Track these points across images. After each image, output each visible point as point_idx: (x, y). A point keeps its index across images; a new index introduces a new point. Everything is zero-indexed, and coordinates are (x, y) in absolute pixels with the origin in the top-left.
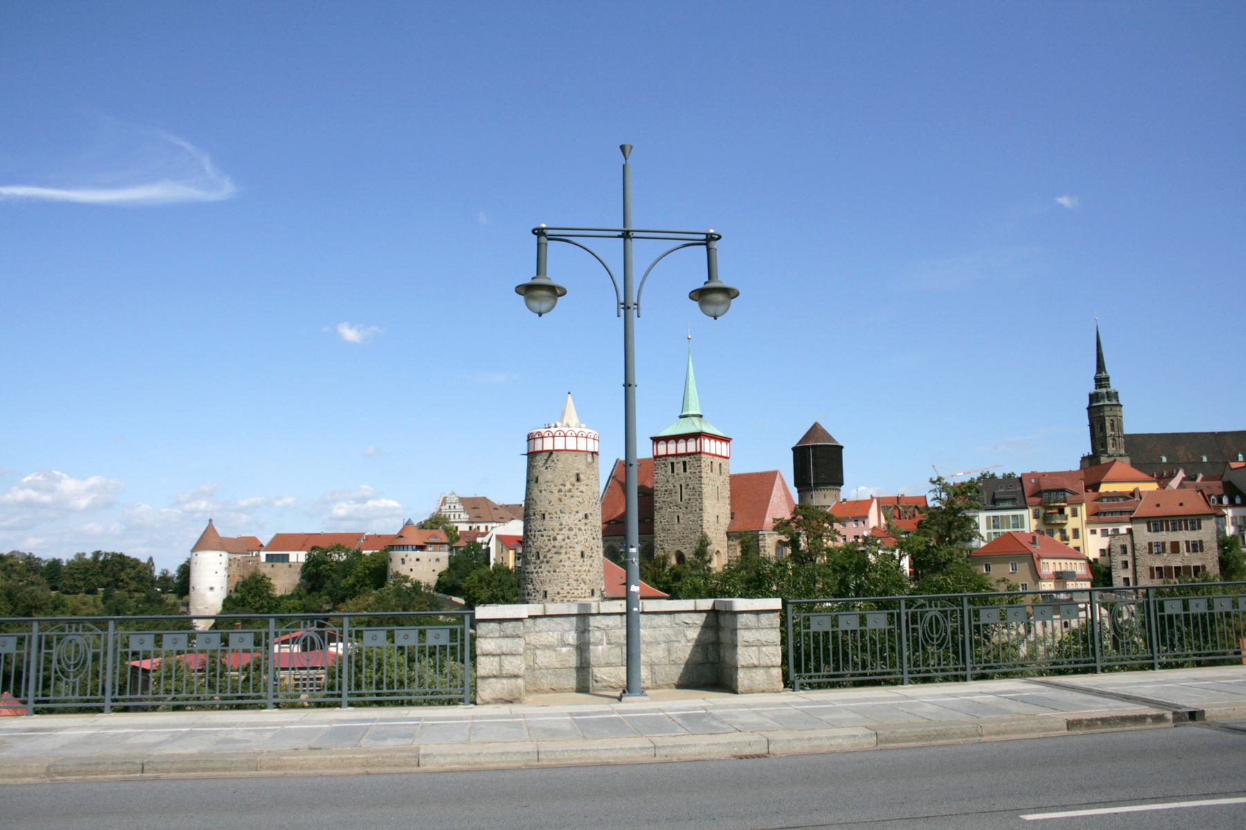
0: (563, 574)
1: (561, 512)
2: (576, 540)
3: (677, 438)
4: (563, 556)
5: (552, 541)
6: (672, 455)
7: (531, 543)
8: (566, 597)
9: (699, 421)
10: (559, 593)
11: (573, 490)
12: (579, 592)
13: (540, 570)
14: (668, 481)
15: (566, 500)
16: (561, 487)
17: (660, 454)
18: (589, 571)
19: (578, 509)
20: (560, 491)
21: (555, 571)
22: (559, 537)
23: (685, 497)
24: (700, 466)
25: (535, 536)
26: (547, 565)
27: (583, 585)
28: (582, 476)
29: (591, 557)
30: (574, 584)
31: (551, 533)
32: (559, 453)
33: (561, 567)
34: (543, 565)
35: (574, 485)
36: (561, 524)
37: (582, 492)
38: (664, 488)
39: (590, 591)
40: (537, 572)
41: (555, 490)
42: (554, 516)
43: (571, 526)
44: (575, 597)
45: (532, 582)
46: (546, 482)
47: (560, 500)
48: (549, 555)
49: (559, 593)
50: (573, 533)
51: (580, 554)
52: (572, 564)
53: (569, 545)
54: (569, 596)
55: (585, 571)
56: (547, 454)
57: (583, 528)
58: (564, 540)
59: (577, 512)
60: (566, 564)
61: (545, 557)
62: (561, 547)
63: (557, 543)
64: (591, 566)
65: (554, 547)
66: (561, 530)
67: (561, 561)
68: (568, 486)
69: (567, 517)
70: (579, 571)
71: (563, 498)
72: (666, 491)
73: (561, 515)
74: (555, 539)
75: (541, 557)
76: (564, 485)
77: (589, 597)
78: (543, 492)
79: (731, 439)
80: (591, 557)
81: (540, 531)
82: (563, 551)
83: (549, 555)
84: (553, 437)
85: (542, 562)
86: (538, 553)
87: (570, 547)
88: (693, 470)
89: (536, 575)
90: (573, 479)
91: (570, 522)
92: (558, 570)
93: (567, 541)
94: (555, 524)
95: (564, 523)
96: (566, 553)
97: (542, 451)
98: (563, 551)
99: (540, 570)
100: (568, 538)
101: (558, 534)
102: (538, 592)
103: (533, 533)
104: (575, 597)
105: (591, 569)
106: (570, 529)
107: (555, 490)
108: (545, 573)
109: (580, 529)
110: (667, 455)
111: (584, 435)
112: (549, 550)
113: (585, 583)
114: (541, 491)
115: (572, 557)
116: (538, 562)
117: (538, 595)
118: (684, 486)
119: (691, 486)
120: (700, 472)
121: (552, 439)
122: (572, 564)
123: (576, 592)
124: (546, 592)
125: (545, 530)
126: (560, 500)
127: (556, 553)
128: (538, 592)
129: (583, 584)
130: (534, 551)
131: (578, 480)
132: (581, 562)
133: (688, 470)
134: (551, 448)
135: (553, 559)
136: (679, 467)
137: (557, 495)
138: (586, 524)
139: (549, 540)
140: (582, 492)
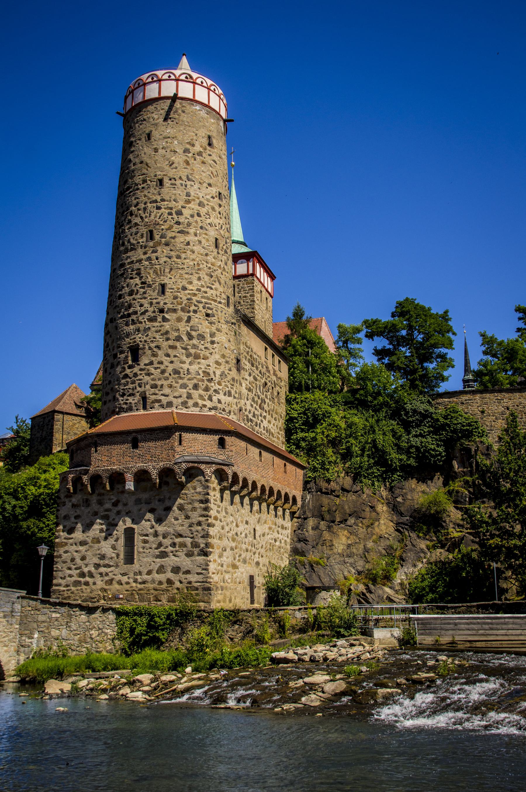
0: (192, 263)
2: (208, 221)
4: (190, 238)
5: (175, 216)
7: (138, 220)
8: (195, 295)
10: (184, 288)
11: (204, 155)
12: (213, 292)
13: (154, 256)
15: (196, 165)
16: (188, 146)
20: (186, 151)
21: (179, 257)
22: (186, 212)
24: (253, 289)
25: (145, 209)
26: (168, 248)
27: (217, 285)
28: (214, 141)
30: (207, 278)
31: (173, 204)
32: (185, 103)
33: (188, 252)
34: (159, 249)
35: (205, 149)
36: (188, 195)
40: (149, 259)
41: (180, 150)
42: (178, 182)
44: (208, 298)
45: (139, 274)
46: (165, 138)
47: (187, 163)
48: (170, 234)
52: (202, 251)
53: (200, 224)
56: (169, 101)
58: (192, 216)
59: (210, 185)
60: (195, 248)
62: (189, 224)
63: (182, 219)
65: (178, 223)
66: (188, 202)
68: (198, 148)
71: (191, 161)
73: (189, 183)
74: (179, 213)
75: (157, 237)
76: (193, 145)
78: (160, 151)
81: (156, 201)
82: (192, 231)
84: (177, 80)
85: (159, 243)
86: (151, 232)
87: (201, 228)
89: (147, 263)
90: (205, 141)
91: (201, 195)
92: (183, 256)
93: (196, 217)
94: (180, 192)
95: (192, 194)
96: (196, 235)
97: (160, 99)
98: (192, 231)
99: (154, 256)
100: (199, 215)
101: (183, 207)
102: (150, 286)
103: (142, 206)
104: (208, 298)
106: (201, 204)
107: (180, 150)
108: (163, 260)
109: (213, 209)
112: (170, 228)
114: (156, 150)
115: (203, 241)
116: (151, 244)
117: (149, 291)
120: (252, 296)
121: (174, 83)
123: (210, 292)
124: (163, 286)
125: (163, 200)
128: (150, 286)
129: (217, 283)
130: (144, 230)
131: (210, 144)
132: (216, 253)
133: (237, 294)
135: (177, 240)
139: (170, 214)
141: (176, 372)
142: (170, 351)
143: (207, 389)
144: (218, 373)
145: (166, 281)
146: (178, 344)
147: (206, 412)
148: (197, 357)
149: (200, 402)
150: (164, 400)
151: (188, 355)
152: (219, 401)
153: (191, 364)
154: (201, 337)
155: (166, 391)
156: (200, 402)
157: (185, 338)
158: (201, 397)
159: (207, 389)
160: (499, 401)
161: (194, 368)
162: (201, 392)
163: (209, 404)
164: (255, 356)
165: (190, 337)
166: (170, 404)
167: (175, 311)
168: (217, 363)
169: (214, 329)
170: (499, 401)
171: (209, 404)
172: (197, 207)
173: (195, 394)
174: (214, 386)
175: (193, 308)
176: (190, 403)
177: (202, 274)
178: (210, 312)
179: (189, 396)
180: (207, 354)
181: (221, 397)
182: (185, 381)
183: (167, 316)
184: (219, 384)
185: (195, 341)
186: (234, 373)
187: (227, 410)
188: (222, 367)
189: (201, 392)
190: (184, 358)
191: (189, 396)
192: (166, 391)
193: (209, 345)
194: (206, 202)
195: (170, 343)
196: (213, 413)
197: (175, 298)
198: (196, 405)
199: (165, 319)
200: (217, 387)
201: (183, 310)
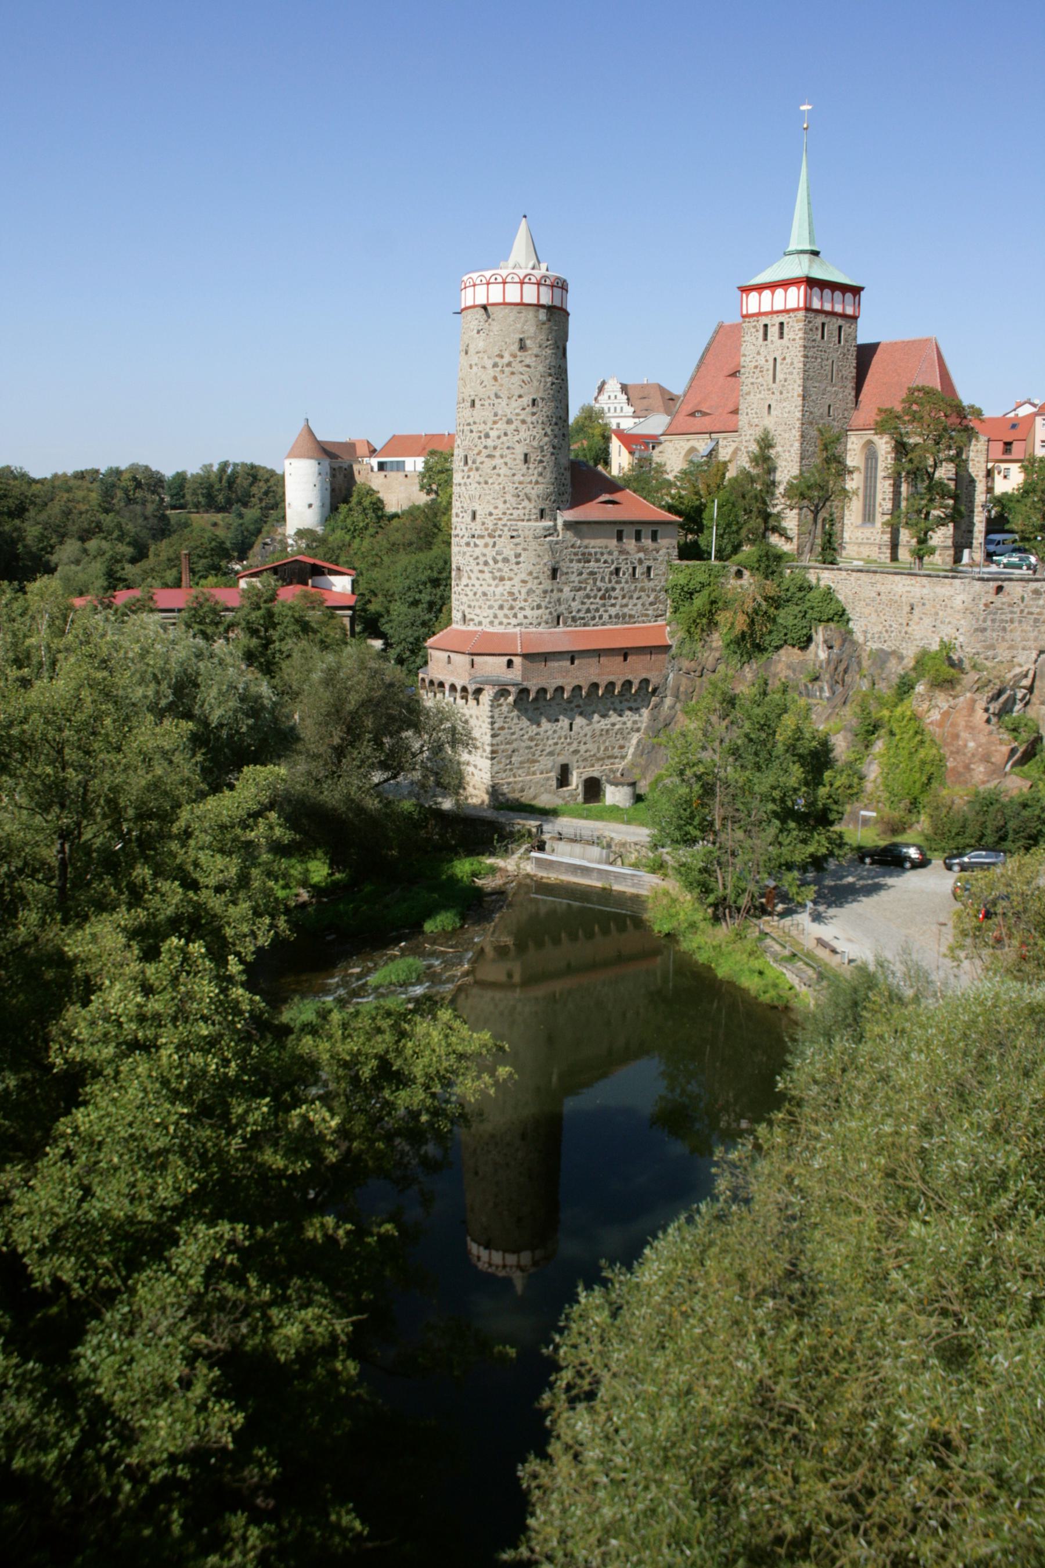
1: (497, 396)
2: (516, 438)
3: (772, 286)
4: (498, 461)
6: (766, 314)
9: (810, 261)
10: (491, 514)
12: (521, 512)
14: (759, 353)
16: (497, 360)
17: (750, 312)
18: (537, 483)
19: (522, 392)
21: (486, 483)
22: (493, 434)
23: (780, 376)
27: (526, 503)
29: (541, 462)
30: (513, 501)
31: (482, 427)
35: (515, 356)
36: (496, 415)
37: (528, 366)
38: (753, 364)
39: (537, 511)
43: (509, 416)
47: (495, 379)
48: (479, 459)
49: (491, 514)
50: (513, 427)
51: (522, 457)
54: (505, 518)
55: (531, 482)
57: (529, 419)
58: (499, 437)
59: (520, 396)
60: (501, 472)
61: (474, 462)
62: (495, 448)
63: (489, 443)
64: (540, 474)
65: (486, 447)
66: (495, 423)
67: (494, 468)
69: (504, 403)
70: (520, 483)
72: (756, 367)
73: (497, 401)
74: (487, 436)
75: (470, 462)
76: (502, 357)
77: (536, 520)
79: (862, 289)
80: (541, 462)
83: (479, 459)
85: (470, 470)
88: (792, 336)
90: (516, 346)
91: (508, 412)
93: (504, 438)
95: (500, 412)
96: (502, 456)
98: (497, 453)
100: (506, 434)
105: (540, 479)
110: (760, 314)
111: (534, 280)
113: (529, 499)
116: (466, 468)
118: (779, 361)
119: (788, 360)
122: (509, 473)
123: (516, 513)
126: (495, 379)
127: (489, 456)
134: (484, 302)
136: (773, 331)
137: (491, 372)
138: (534, 414)
140: (528, 366)
141: (485, 594)
142: (480, 575)
143: (512, 608)
144: (524, 591)
145: (477, 507)
146: (486, 569)
147: (511, 630)
148: (502, 579)
149: (505, 621)
150: (477, 619)
151: (494, 579)
152: (525, 617)
153: (497, 586)
154: (506, 560)
155: (478, 611)
156: (505, 621)
157: (491, 562)
158: (506, 616)
159: (512, 608)
160: (873, 584)
161: (500, 589)
162: (506, 611)
163: (514, 621)
164: (593, 551)
165: (496, 562)
166: (480, 623)
167: (481, 537)
168: (524, 582)
169: (519, 550)
170: (873, 584)
171: (514, 621)
172: (505, 426)
173: (500, 613)
174: (518, 604)
175: (499, 533)
176: (496, 622)
177: (508, 497)
178: (514, 534)
179: (495, 617)
180: (512, 575)
181: (528, 612)
182: (491, 603)
183: (478, 542)
184: (525, 601)
185: (500, 565)
186: (547, 584)
187: (535, 622)
188: (529, 585)
189: (506, 611)
190: (491, 582)
191: (495, 617)
192: (478, 611)
193: (514, 567)
194: (514, 418)
195: (481, 567)
196: (518, 629)
197: (483, 524)
198: (501, 623)
199: (476, 545)
200: (523, 604)
201: (490, 536)
